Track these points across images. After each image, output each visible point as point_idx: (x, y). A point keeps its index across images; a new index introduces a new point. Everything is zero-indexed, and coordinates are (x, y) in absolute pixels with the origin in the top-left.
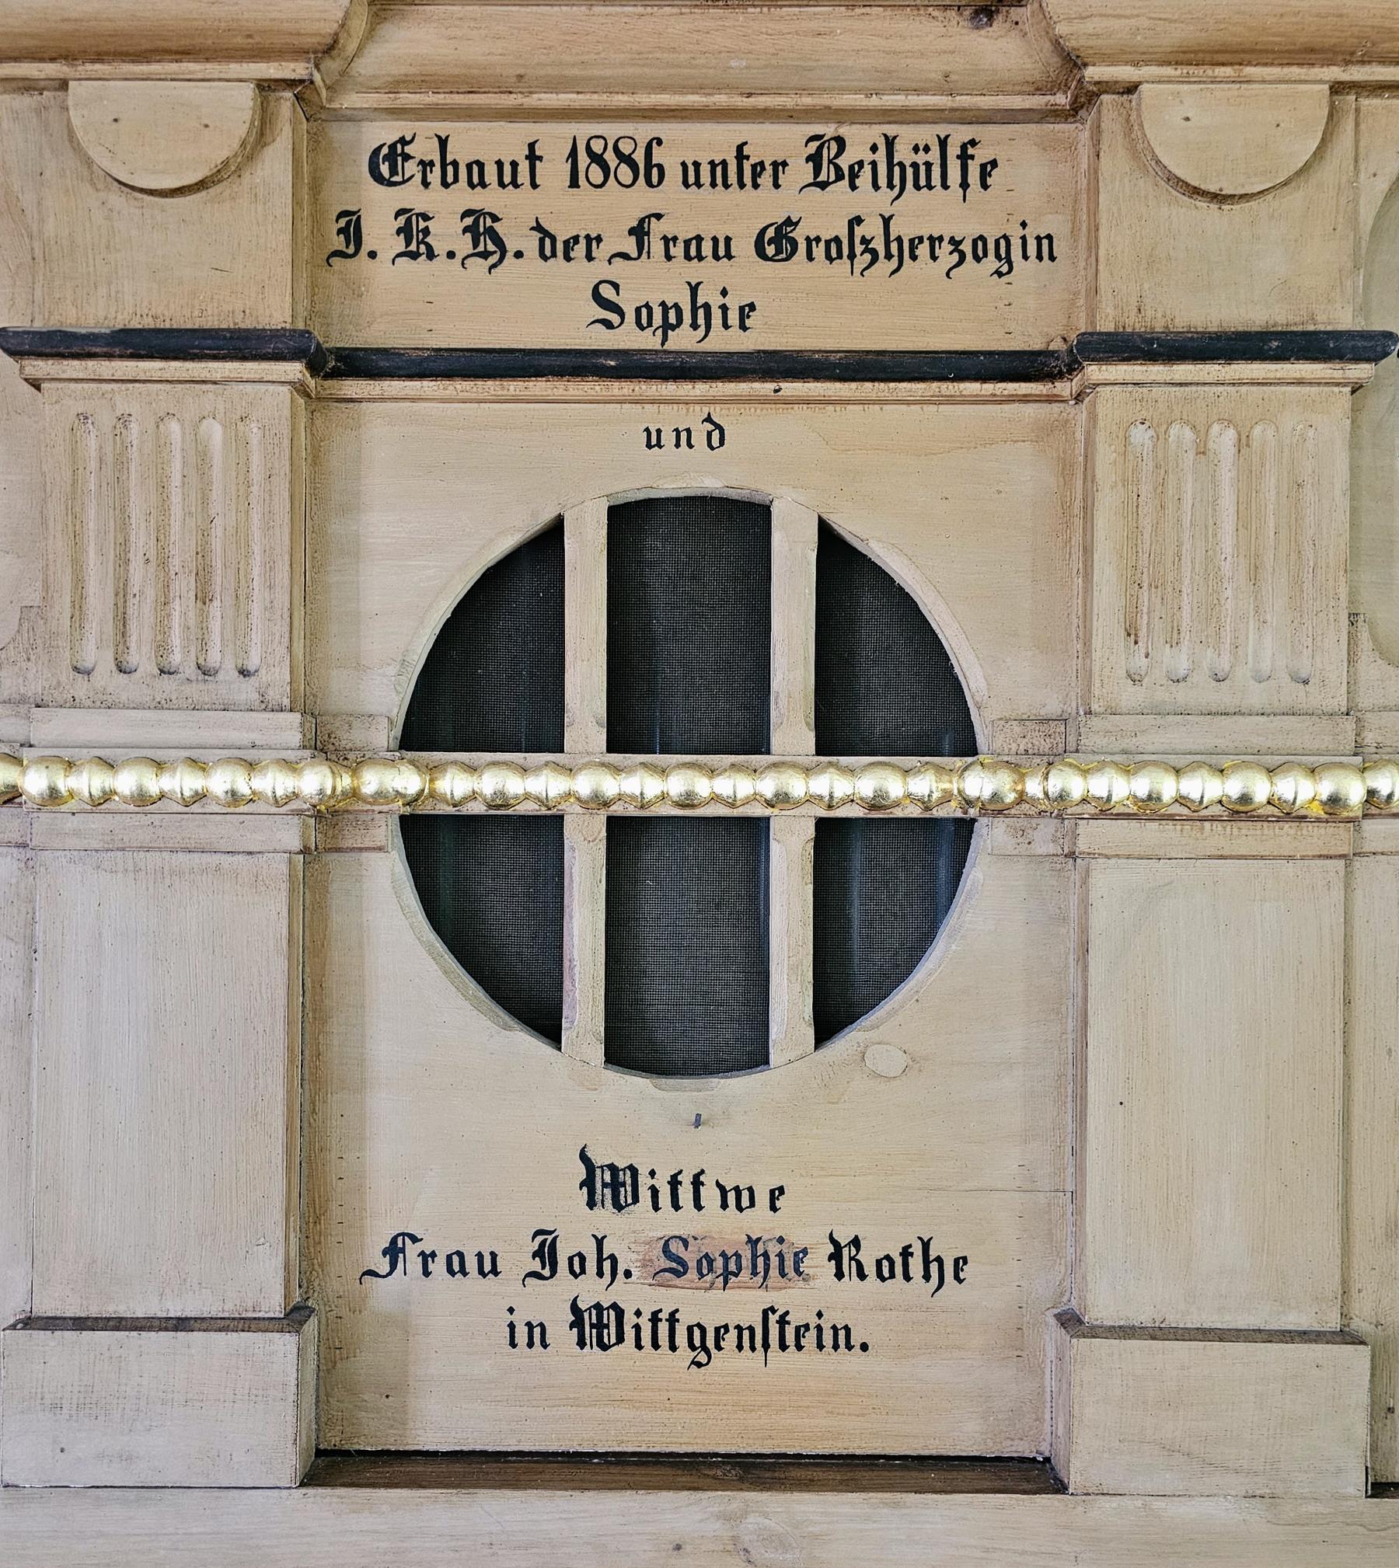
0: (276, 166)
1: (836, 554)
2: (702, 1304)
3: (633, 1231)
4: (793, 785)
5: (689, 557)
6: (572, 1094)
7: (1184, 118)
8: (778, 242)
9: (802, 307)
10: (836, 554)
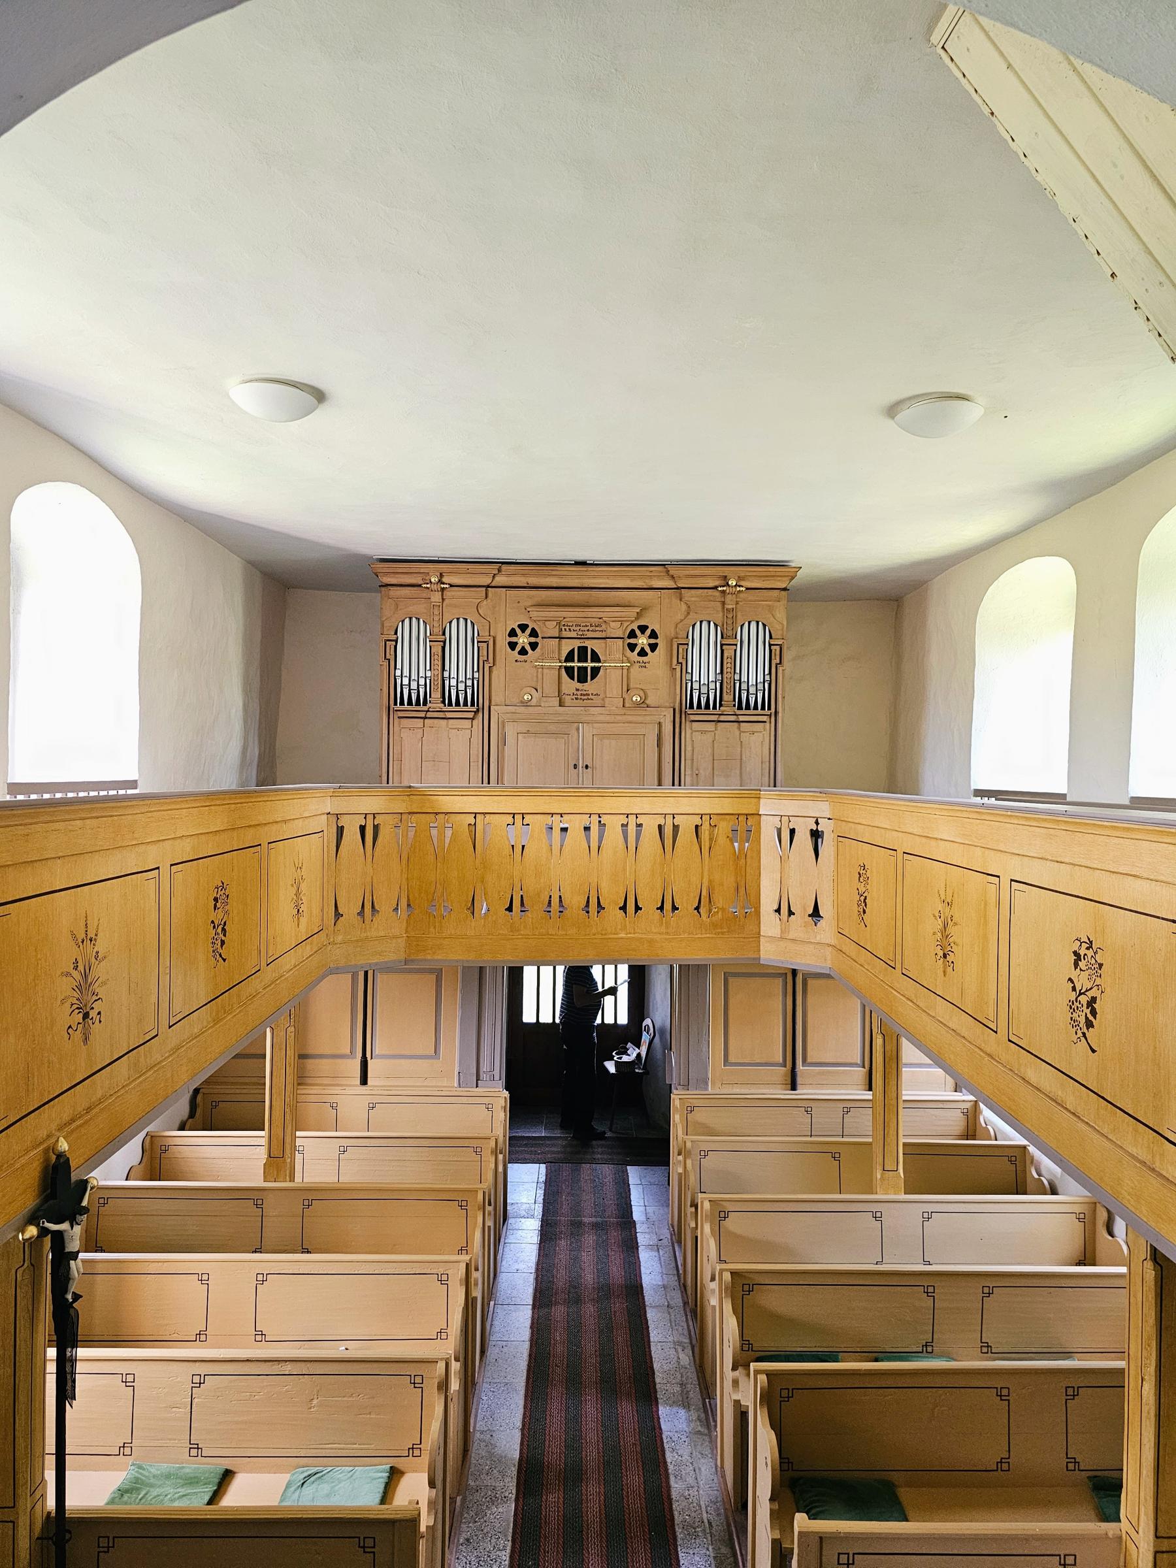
4: (590, 665)
5: (583, 650)
6: (575, 684)
7: (612, 624)
9: (590, 635)
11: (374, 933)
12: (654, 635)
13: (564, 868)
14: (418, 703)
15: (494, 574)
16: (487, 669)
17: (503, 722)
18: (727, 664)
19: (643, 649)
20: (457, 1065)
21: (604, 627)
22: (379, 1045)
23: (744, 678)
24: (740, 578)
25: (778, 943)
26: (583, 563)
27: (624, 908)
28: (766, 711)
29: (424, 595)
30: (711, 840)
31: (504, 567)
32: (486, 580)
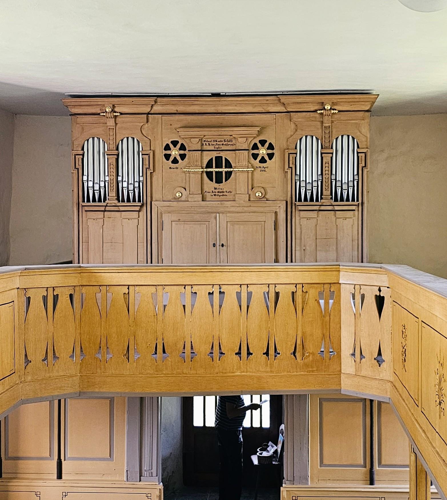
0: (200, 142)
1: (226, 159)
2: (219, 194)
3: (217, 191)
4: (224, 170)
5: (219, 159)
6: (214, 184)
7: (240, 140)
8: (223, 145)
9: (224, 148)
10: (226, 159)
11: (55, 374)
12: (271, 147)
13: (197, 324)
14: (100, 200)
15: (153, 104)
16: (149, 174)
17: (161, 214)
18: (326, 167)
19: (263, 157)
20: (126, 465)
21: (234, 142)
22: (70, 451)
23: (339, 178)
24: (333, 104)
25: (355, 378)
26: (217, 95)
27: (239, 353)
28: (356, 203)
29: (102, 121)
30: (303, 302)
31: (159, 99)
32: (147, 109)
